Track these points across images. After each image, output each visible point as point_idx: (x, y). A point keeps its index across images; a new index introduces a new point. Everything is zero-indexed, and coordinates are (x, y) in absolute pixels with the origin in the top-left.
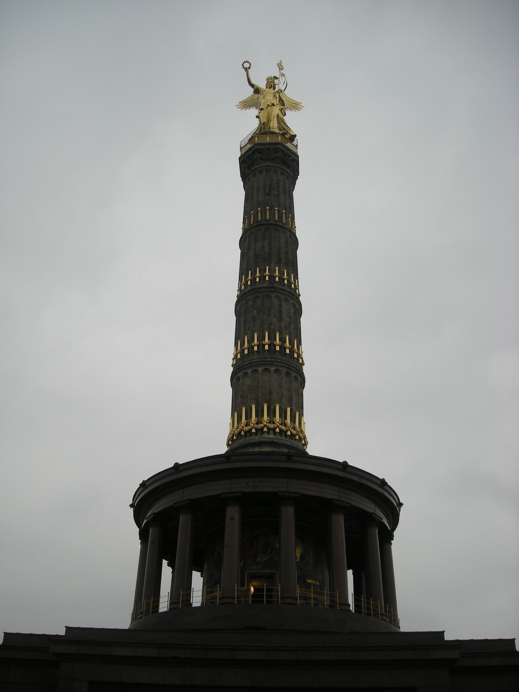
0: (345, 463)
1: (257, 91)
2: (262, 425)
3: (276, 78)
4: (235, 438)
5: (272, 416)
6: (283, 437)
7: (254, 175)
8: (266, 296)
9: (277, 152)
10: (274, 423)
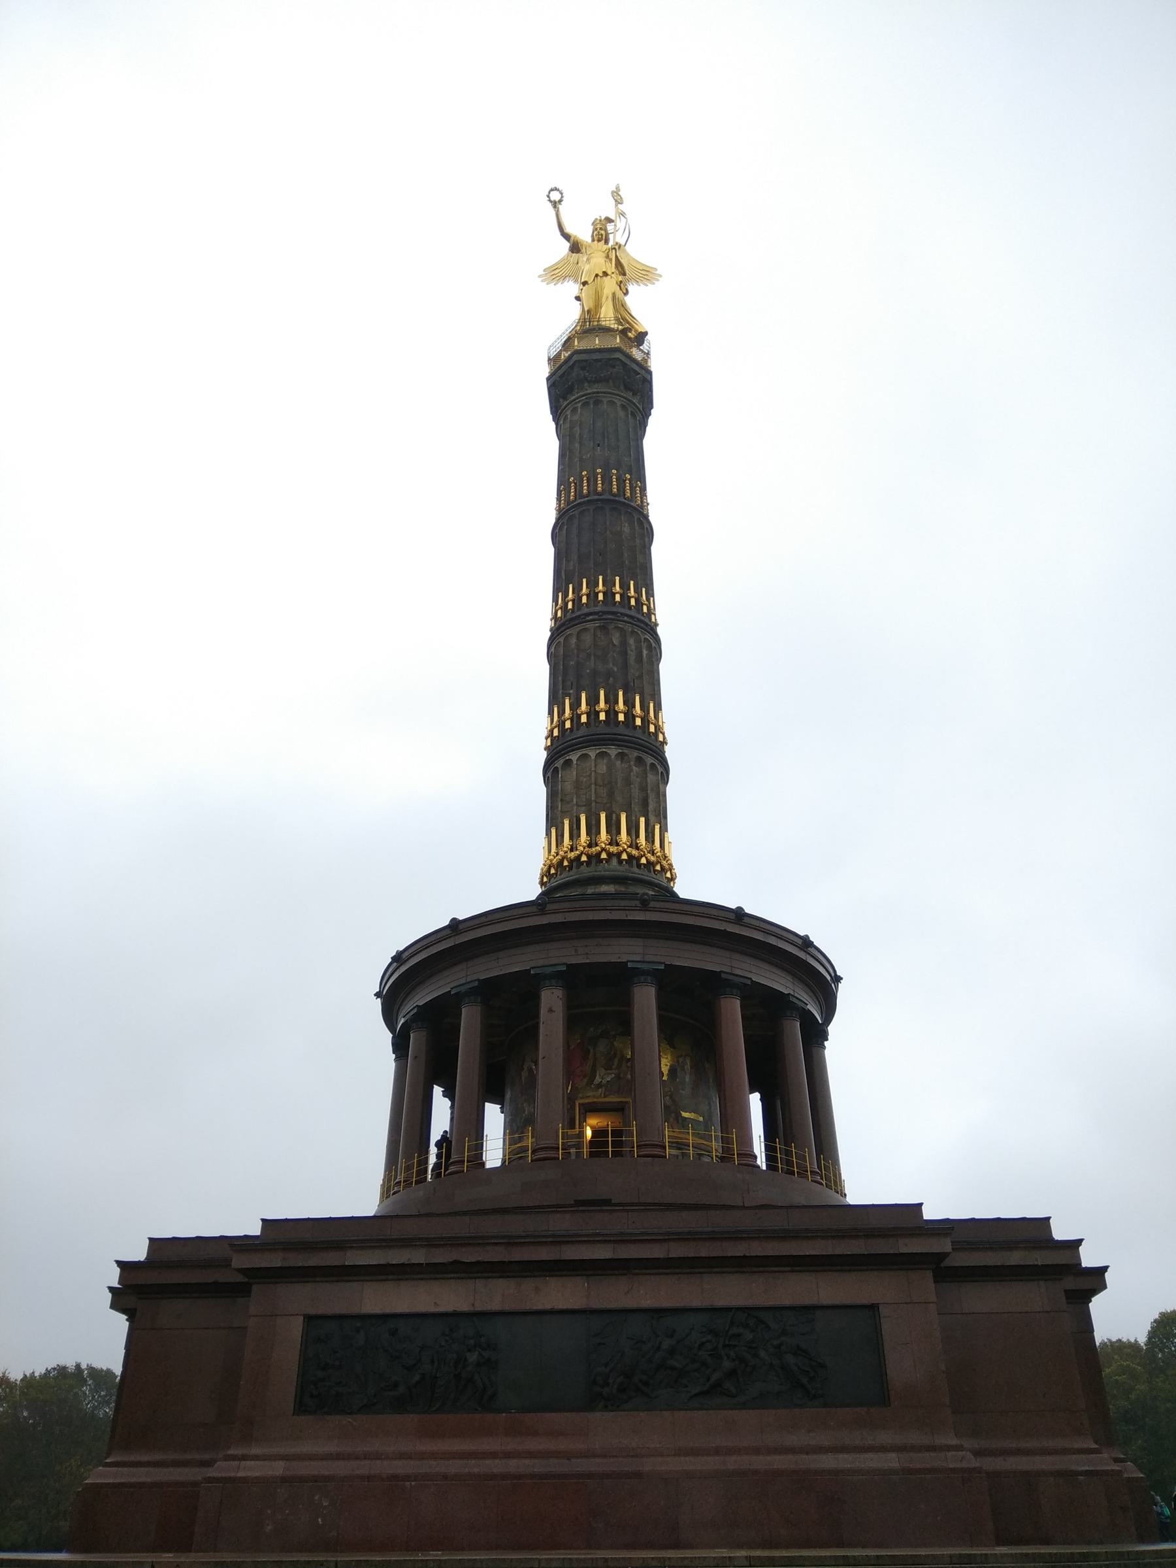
0: (740, 909)
1: (576, 248)
2: (598, 848)
3: (609, 220)
4: (553, 871)
5: (614, 832)
6: (635, 869)
7: (574, 410)
9: (614, 367)
10: (618, 845)
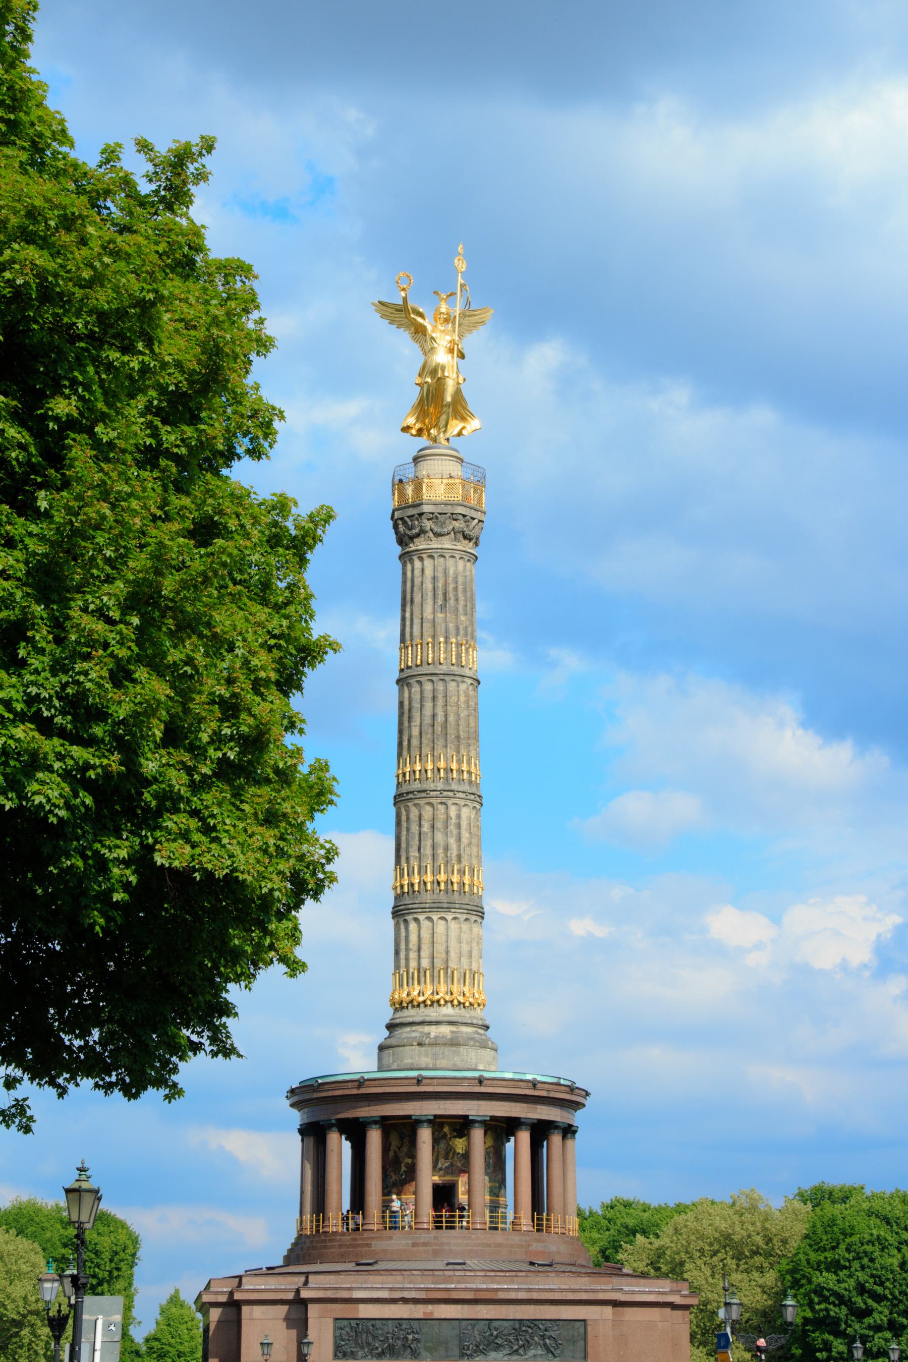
5: (449, 983)
8: (441, 803)
9: (456, 520)
